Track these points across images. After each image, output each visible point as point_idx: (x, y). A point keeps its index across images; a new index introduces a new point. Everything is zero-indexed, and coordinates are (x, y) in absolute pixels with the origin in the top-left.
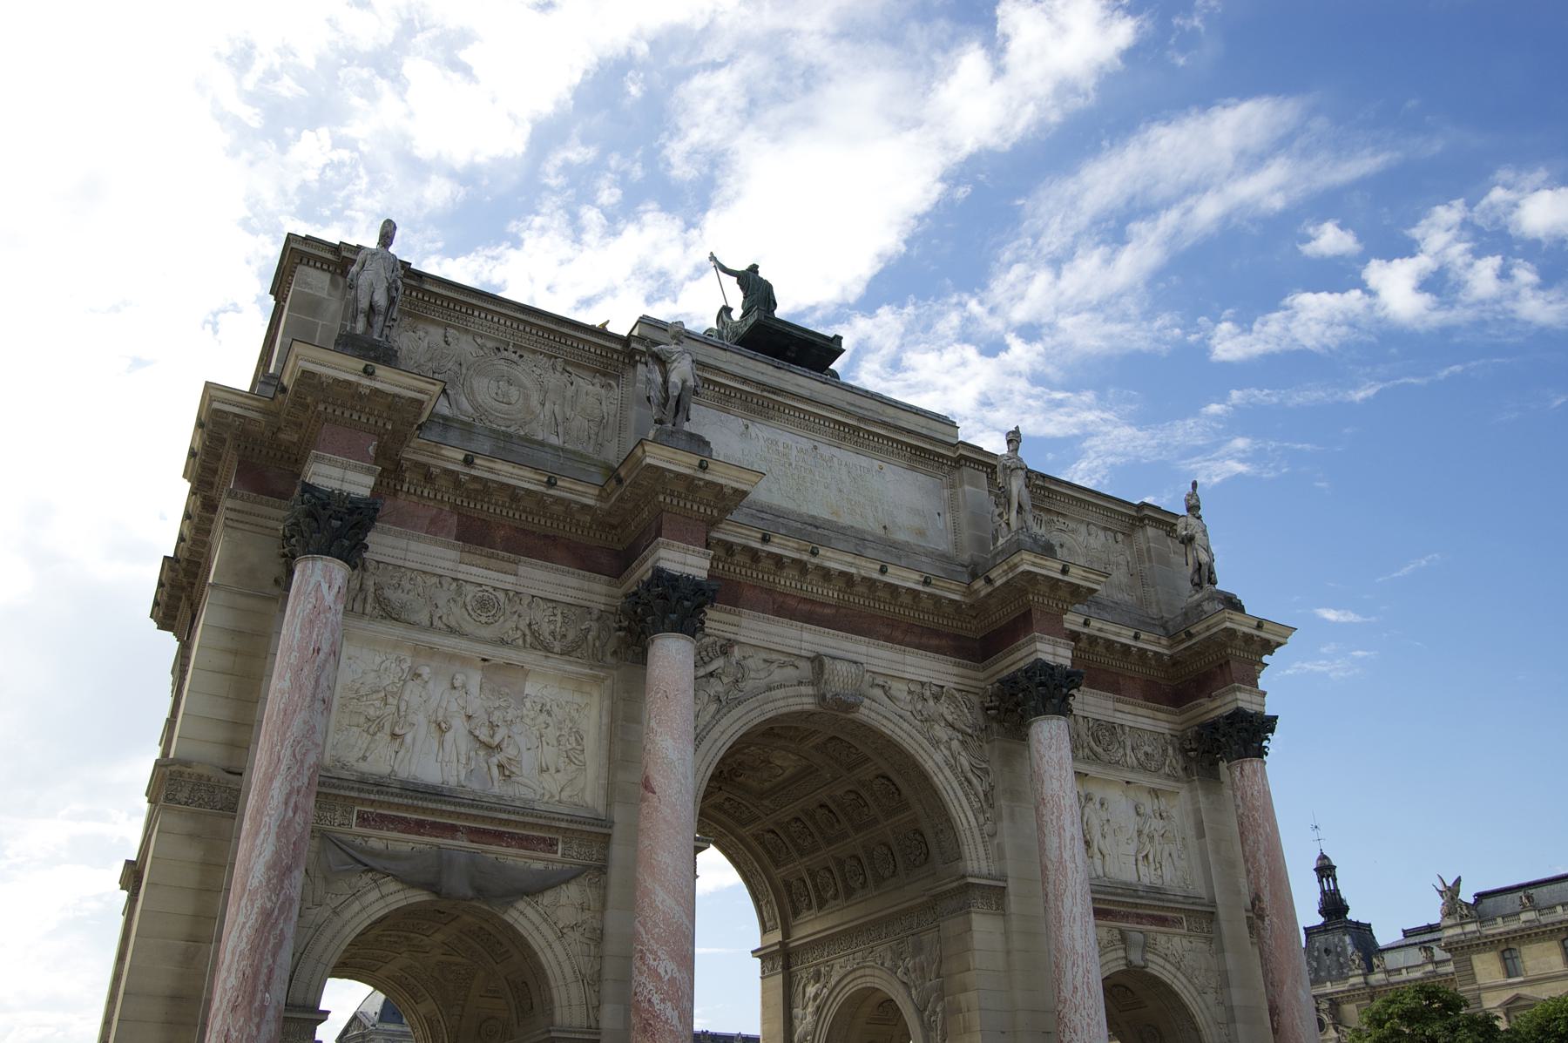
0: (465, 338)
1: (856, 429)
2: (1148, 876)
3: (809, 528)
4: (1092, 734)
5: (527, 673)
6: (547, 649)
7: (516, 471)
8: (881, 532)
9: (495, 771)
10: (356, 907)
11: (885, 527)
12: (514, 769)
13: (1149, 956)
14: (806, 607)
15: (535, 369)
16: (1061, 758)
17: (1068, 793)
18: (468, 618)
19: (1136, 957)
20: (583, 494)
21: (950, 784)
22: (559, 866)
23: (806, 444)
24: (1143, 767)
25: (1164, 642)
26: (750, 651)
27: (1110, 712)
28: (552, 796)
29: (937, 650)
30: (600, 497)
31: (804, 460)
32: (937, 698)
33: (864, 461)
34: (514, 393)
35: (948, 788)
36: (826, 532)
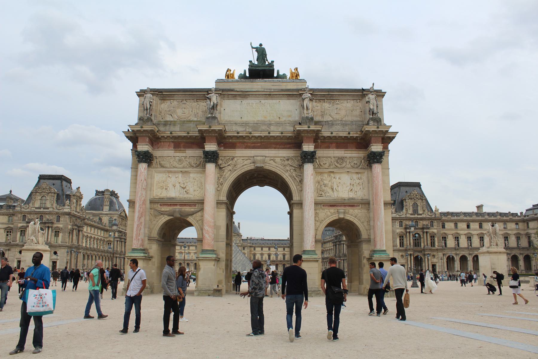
0: (175, 101)
1: (270, 94)
2: (352, 195)
3: (255, 125)
4: (336, 161)
5: (190, 172)
6: (193, 167)
7: (181, 133)
8: (278, 120)
9: (185, 192)
10: (160, 220)
11: (279, 118)
12: (188, 192)
13: (346, 215)
15: (190, 103)
16: (308, 174)
17: (308, 182)
18: (177, 164)
19: (342, 216)
20: (195, 134)
21: (290, 180)
22: (196, 209)
23: (258, 101)
24: (353, 167)
25: (359, 133)
26: (239, 158)
27: (343, 154)
28: (196, 196)
29: (289, 148)
30: (199, 133)
31: (257, 106)
33: (274, 101)
34: (186, 110)
35: (289, 181)
36: (260, 125)
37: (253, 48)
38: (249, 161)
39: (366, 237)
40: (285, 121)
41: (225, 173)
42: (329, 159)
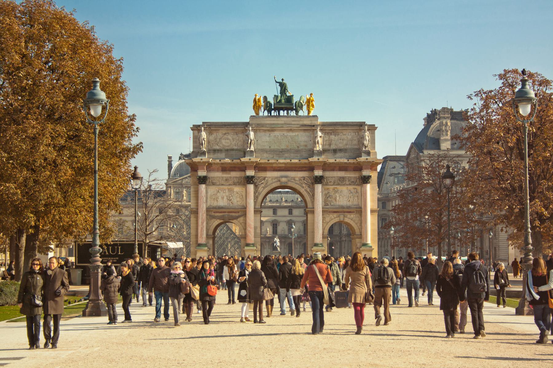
2: (349, 204)
6: (236, 185)
8: (297, 148)
14: (279, 168)
24: (350, 184)
32: (304, 179)
33: (294, 134)
37: (276, 82)
38: (276, 180)
39: (359, 234)
40: (302, 149)
41: (259, 189)
42: (334, 178)
